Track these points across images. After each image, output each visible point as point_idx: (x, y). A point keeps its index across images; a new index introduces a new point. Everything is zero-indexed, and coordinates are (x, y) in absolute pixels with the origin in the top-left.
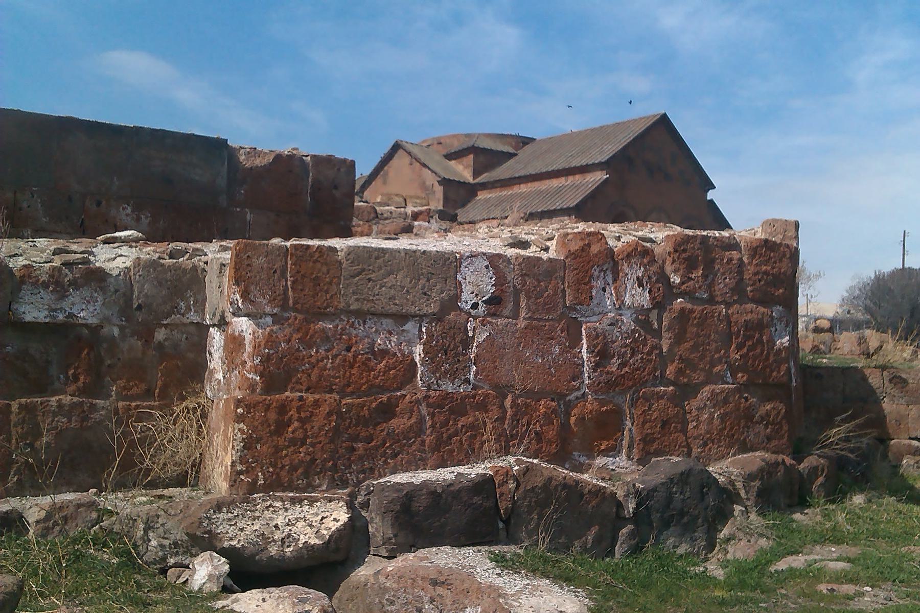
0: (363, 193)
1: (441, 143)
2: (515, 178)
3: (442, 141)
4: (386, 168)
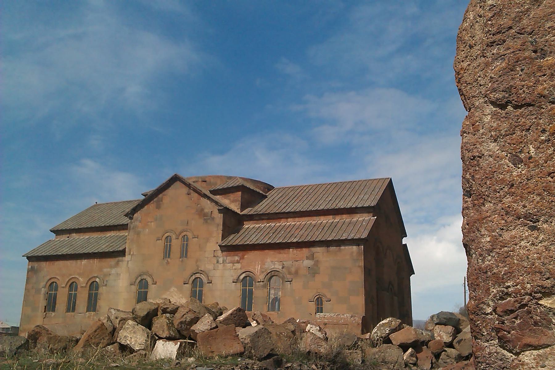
0: (133, 215)
1: (205, 181)
2: (284, 213)
3: (207, 179)
4: (160, 196)
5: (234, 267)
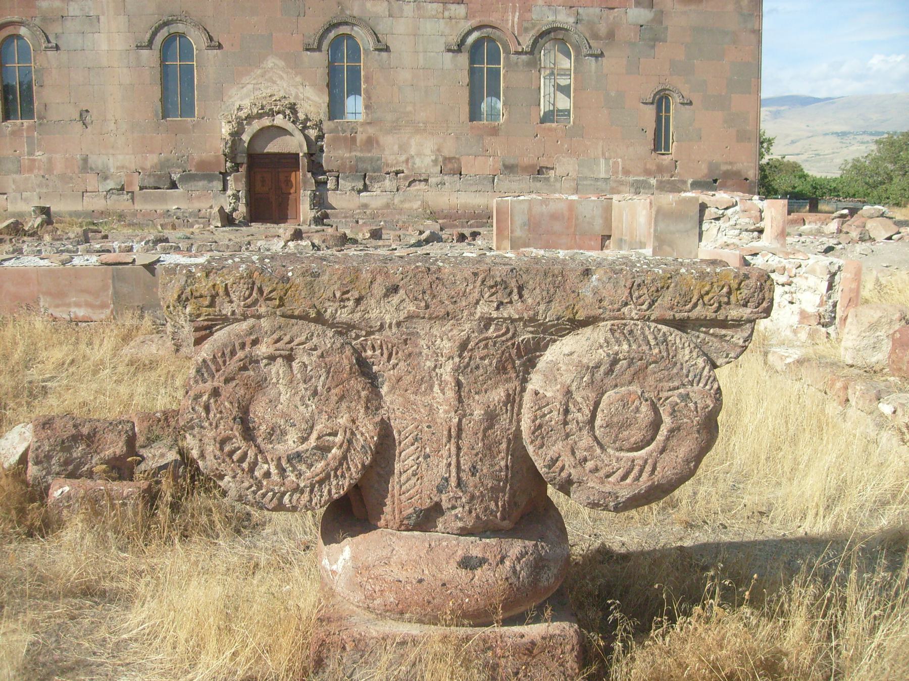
5: (447, 14)
